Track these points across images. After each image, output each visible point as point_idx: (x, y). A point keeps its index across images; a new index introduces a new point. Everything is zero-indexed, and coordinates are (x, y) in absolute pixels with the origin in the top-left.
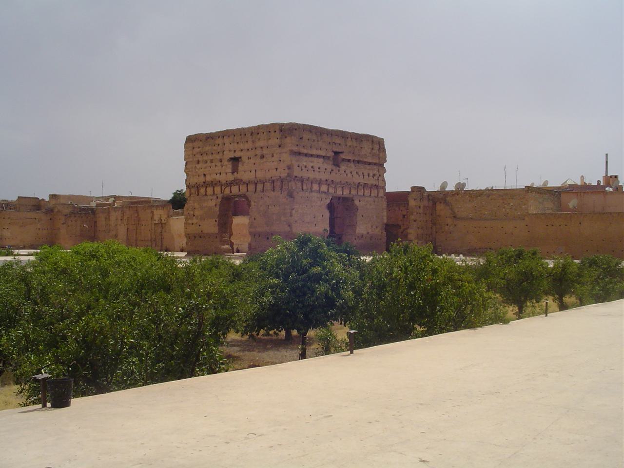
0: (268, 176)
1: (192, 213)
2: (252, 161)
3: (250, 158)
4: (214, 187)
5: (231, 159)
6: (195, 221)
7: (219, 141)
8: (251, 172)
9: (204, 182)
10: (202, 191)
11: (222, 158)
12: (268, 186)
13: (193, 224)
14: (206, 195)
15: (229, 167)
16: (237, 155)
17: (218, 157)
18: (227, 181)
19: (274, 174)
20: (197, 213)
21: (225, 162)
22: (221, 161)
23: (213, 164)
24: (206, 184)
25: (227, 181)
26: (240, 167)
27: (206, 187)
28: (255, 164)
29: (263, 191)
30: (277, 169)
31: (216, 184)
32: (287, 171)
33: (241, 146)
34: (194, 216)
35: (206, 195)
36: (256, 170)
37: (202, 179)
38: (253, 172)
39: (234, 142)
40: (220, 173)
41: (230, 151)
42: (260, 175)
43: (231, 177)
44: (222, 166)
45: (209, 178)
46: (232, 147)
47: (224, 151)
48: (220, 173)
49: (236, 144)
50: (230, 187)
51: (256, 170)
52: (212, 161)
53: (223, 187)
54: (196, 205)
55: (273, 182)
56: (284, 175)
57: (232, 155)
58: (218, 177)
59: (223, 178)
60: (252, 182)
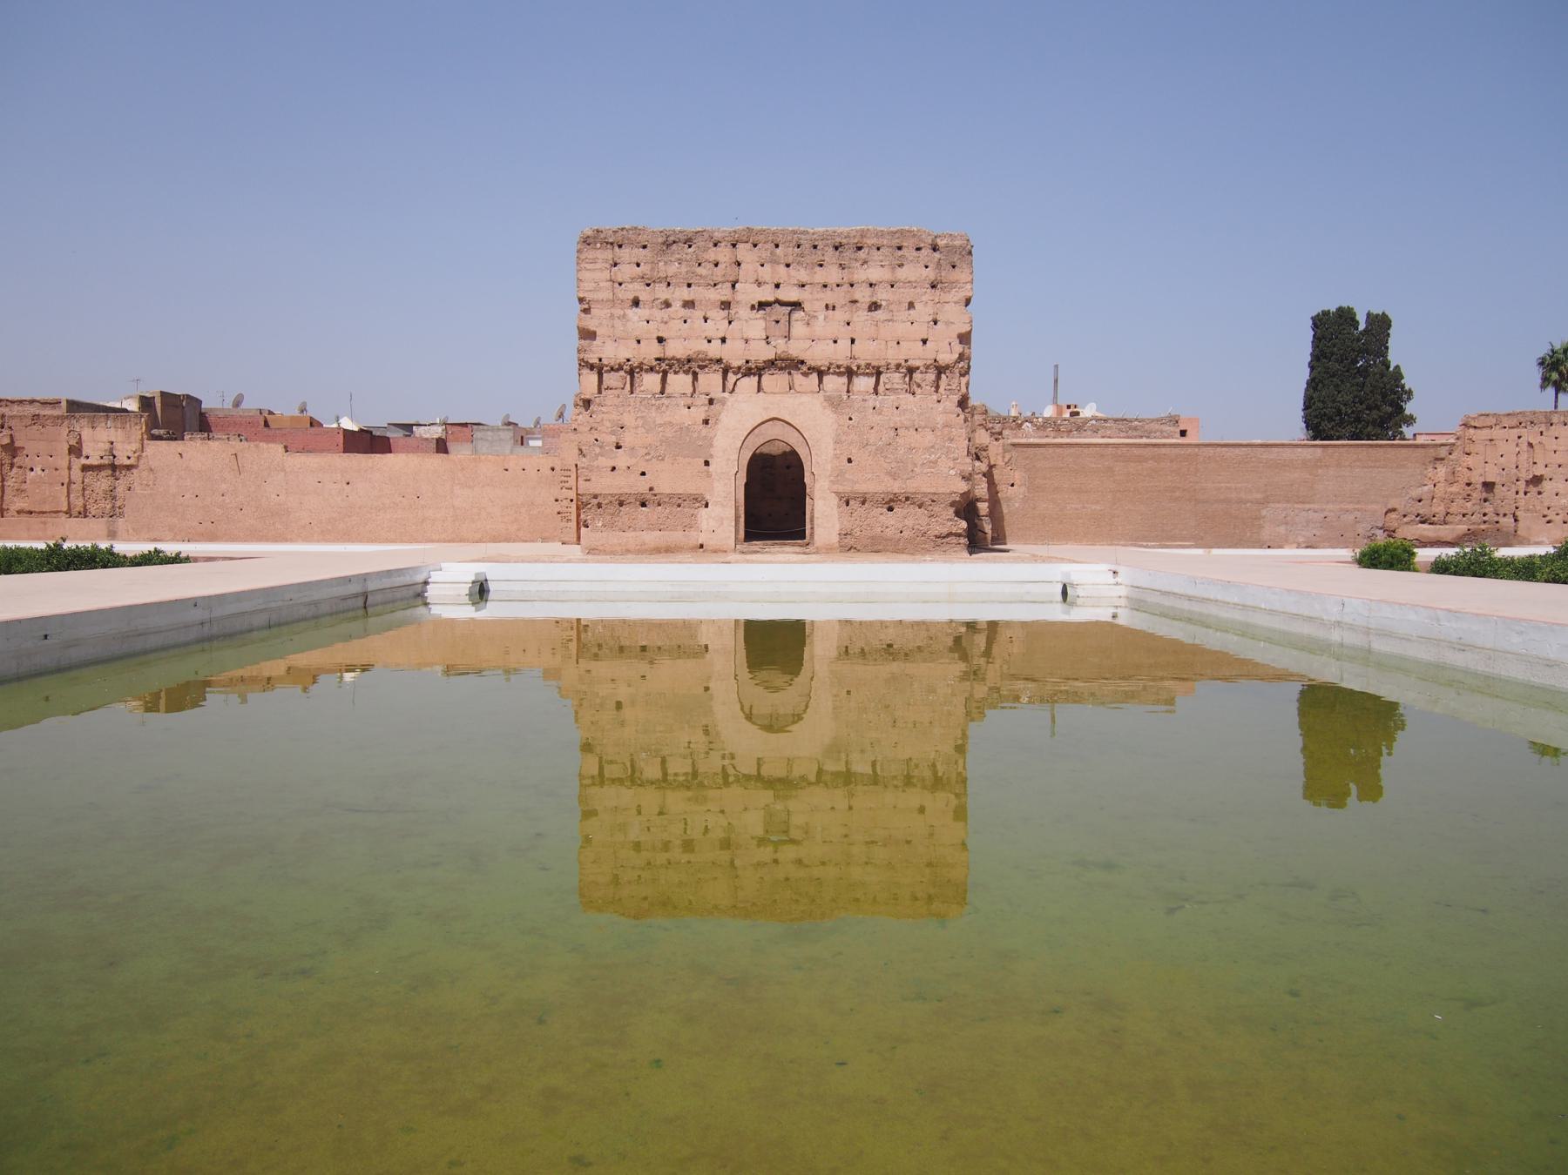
0: (894, 355)
1: (613, 439)
2: (840, 315)
3: (834, 308)
4: (695, 377)
5: (762, 305)
6: (621, 459)
7: (724, 254)
8: (835, 342)
9: (657, 359)
10: (651, 381)
11: (730, 299)
12: (894, 380)
13: (614, 469)
14: (662, 392)
15: (755, 326)
16: (790, 294)
17: (724, 293)
18: (747, 362)
19: (917, 355)
20: (628, 439)
21: (743, 312)
22: (726, 305)
23: (697, 314)
24: (665, 367)
25: (747, 362)
26: (798, 329)
27: (665, 373)
28: (848, 324)
29: (876, 392)
30: (924, 342)
31: (701, 367)
32: (958, 348)
33: (803, 275)
34: (618, 447)
35: (662, 392)
36: (853, 341)
37: (650, 351)
38: (844, 343)
39: (775, 262)
40: (723, 340)
41: (759, 284)
42: (867, 352)
43: (763, 353)
44: (730, 322)
45: (676, 349)
46: (766, 273)
47: (737, 282)
48: (723, 340)
49: (782, 268)
50: (757, 378)
51: (853, 341)
52: (689, 304)
53: (732, 378)
54: (628, 420)
55: (911, 371)
56: (947, 358)
57: (767, 294)
58: (715, 350)
59: (735, 354)
60: (839, 367)
